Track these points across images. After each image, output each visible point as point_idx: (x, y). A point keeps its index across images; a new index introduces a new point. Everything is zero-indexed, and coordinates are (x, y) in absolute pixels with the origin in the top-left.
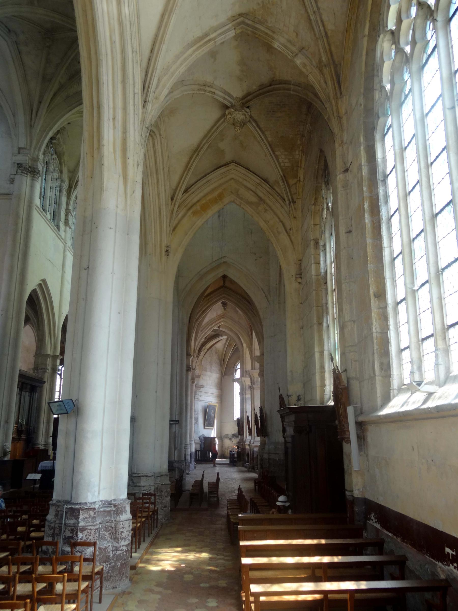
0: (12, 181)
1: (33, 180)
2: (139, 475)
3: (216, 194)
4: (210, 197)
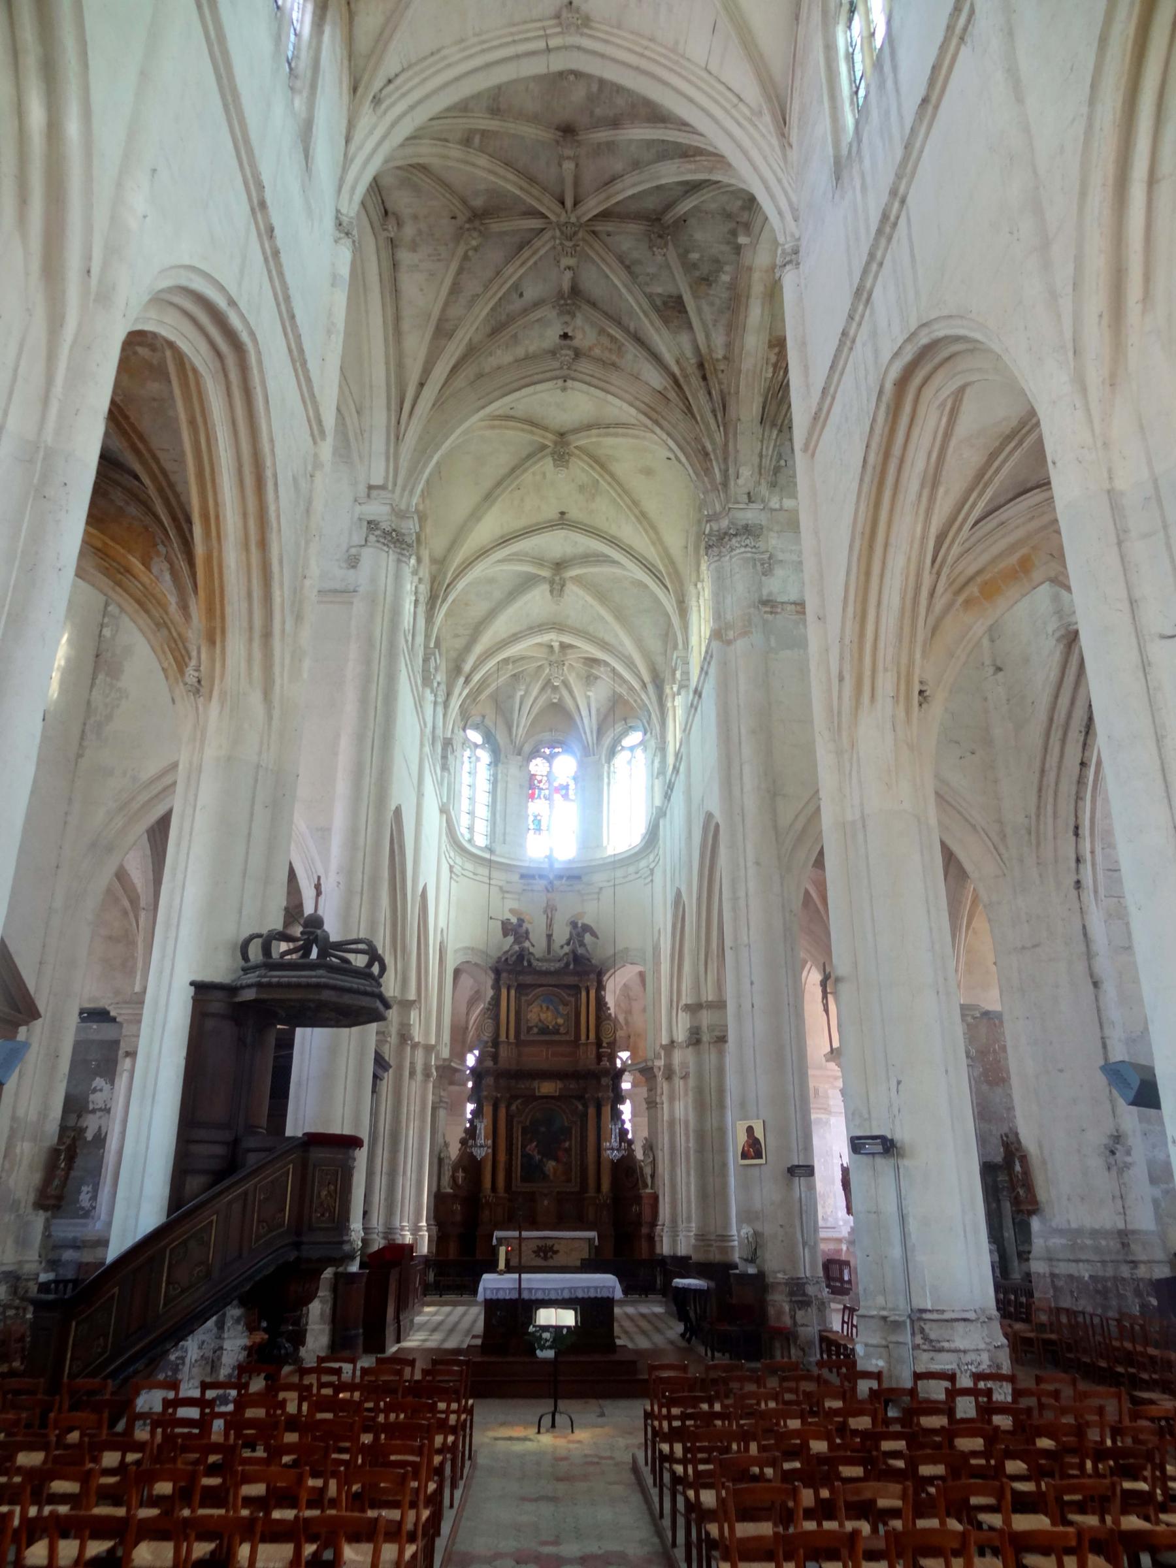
0: (353, 562)
1: (399, 561)
2: (947, 1316)
3: (1013, 559)
4: (1002, 565)
